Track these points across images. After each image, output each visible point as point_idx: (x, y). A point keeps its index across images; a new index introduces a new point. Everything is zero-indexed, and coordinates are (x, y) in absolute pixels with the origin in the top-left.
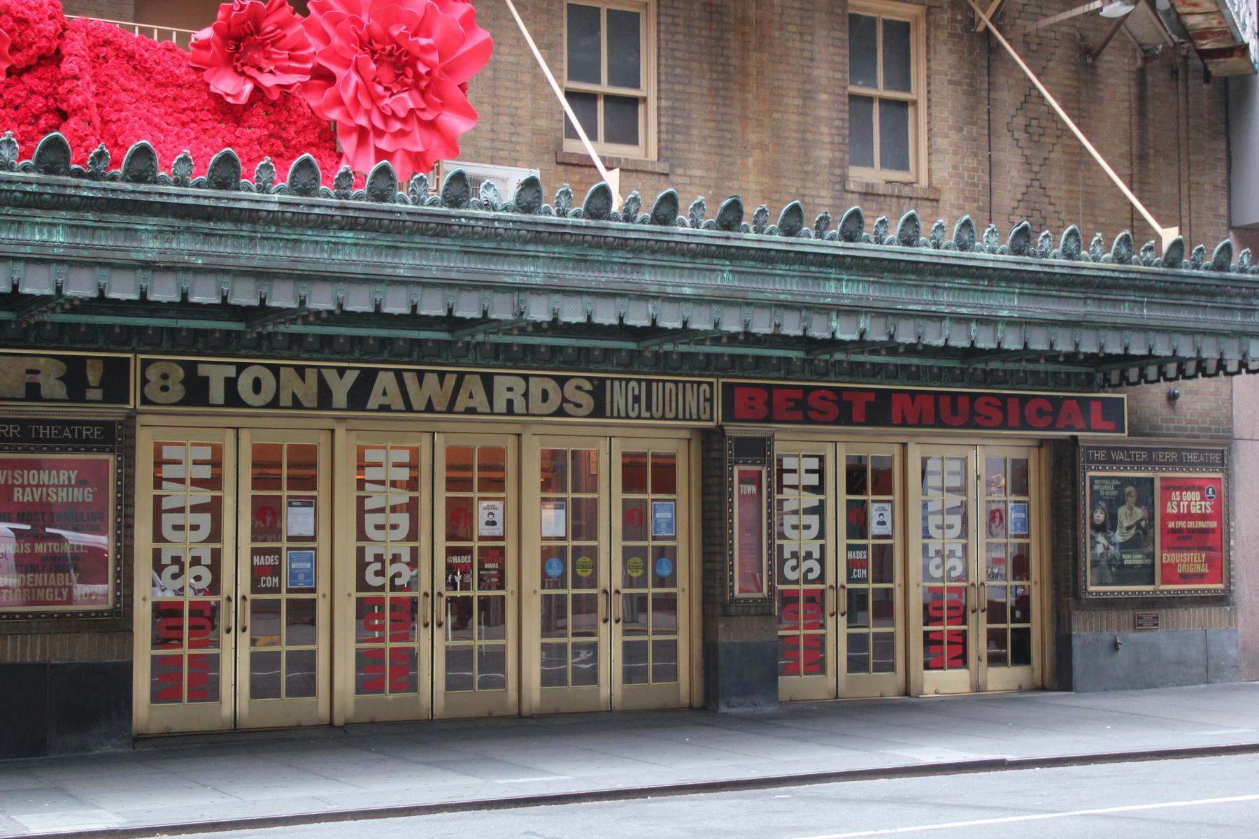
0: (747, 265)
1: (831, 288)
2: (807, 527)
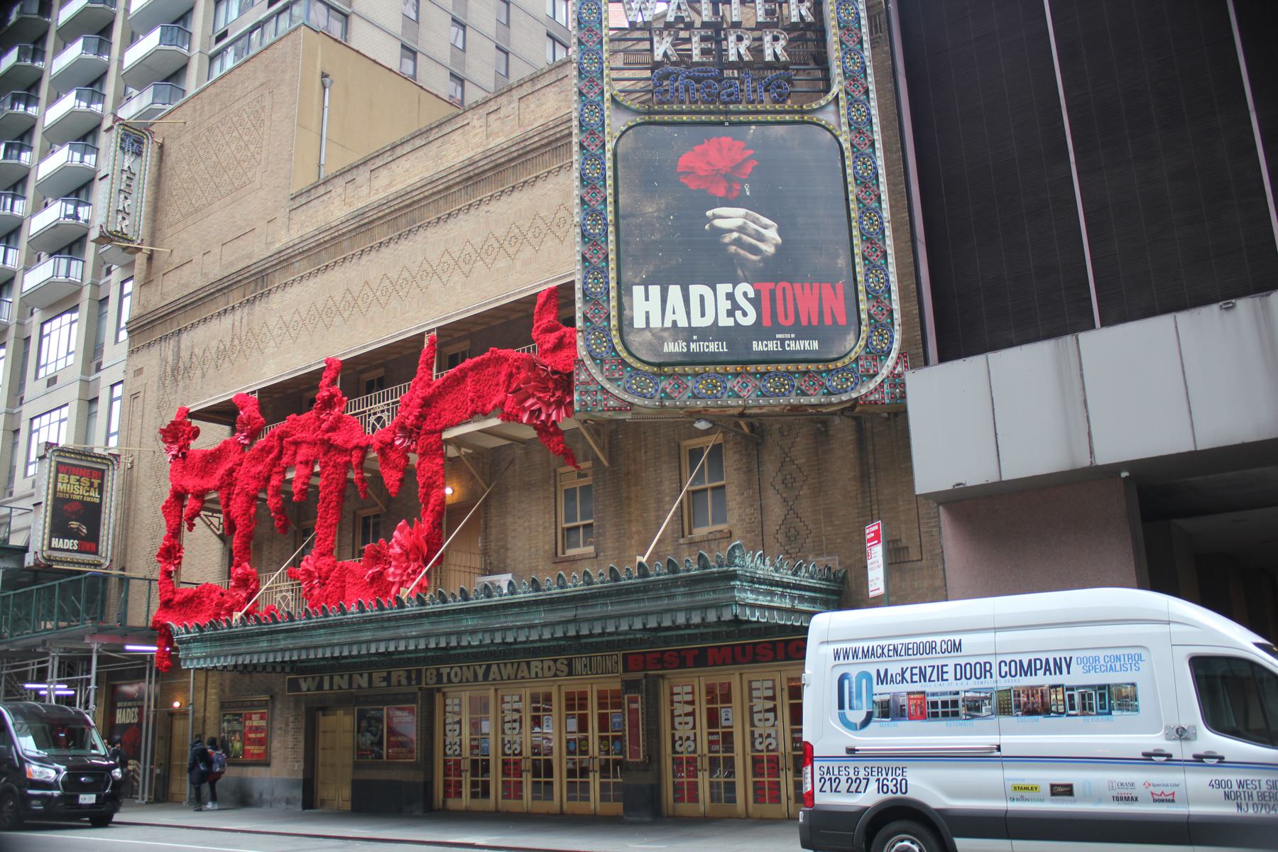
0: (433, 619)
1: (464, 623)
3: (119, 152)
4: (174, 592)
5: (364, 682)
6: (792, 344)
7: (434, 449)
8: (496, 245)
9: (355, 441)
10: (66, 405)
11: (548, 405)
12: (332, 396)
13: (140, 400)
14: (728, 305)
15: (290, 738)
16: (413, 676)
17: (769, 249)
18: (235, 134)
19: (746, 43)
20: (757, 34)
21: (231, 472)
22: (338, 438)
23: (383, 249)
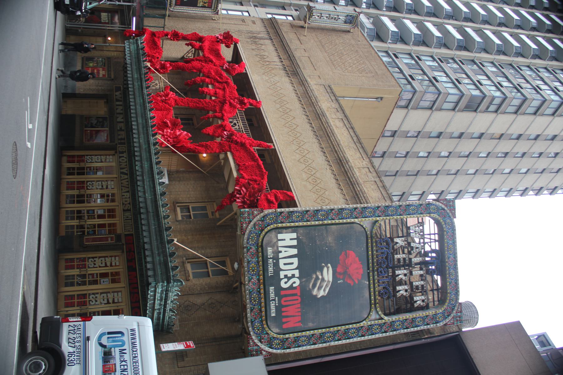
0: (147, 149)
1: (146, 163)
2: (102, 263)
3: (346, 14)
4: (159, 37)
5: (119, 119)
6: (273, 304)
7: (223, 149)
8: (312, 173)
9: (225, 114)
11: (243, 198)
12: (245, 104)
14: (290, 275)
15: (94, 87)
16: (122, 141)
17: (315, 292)
18: (356, 62)
19: (404, 278)
20: (408, 282)
21: (211, 61)
22: (227, 107)
23: (309, 125)
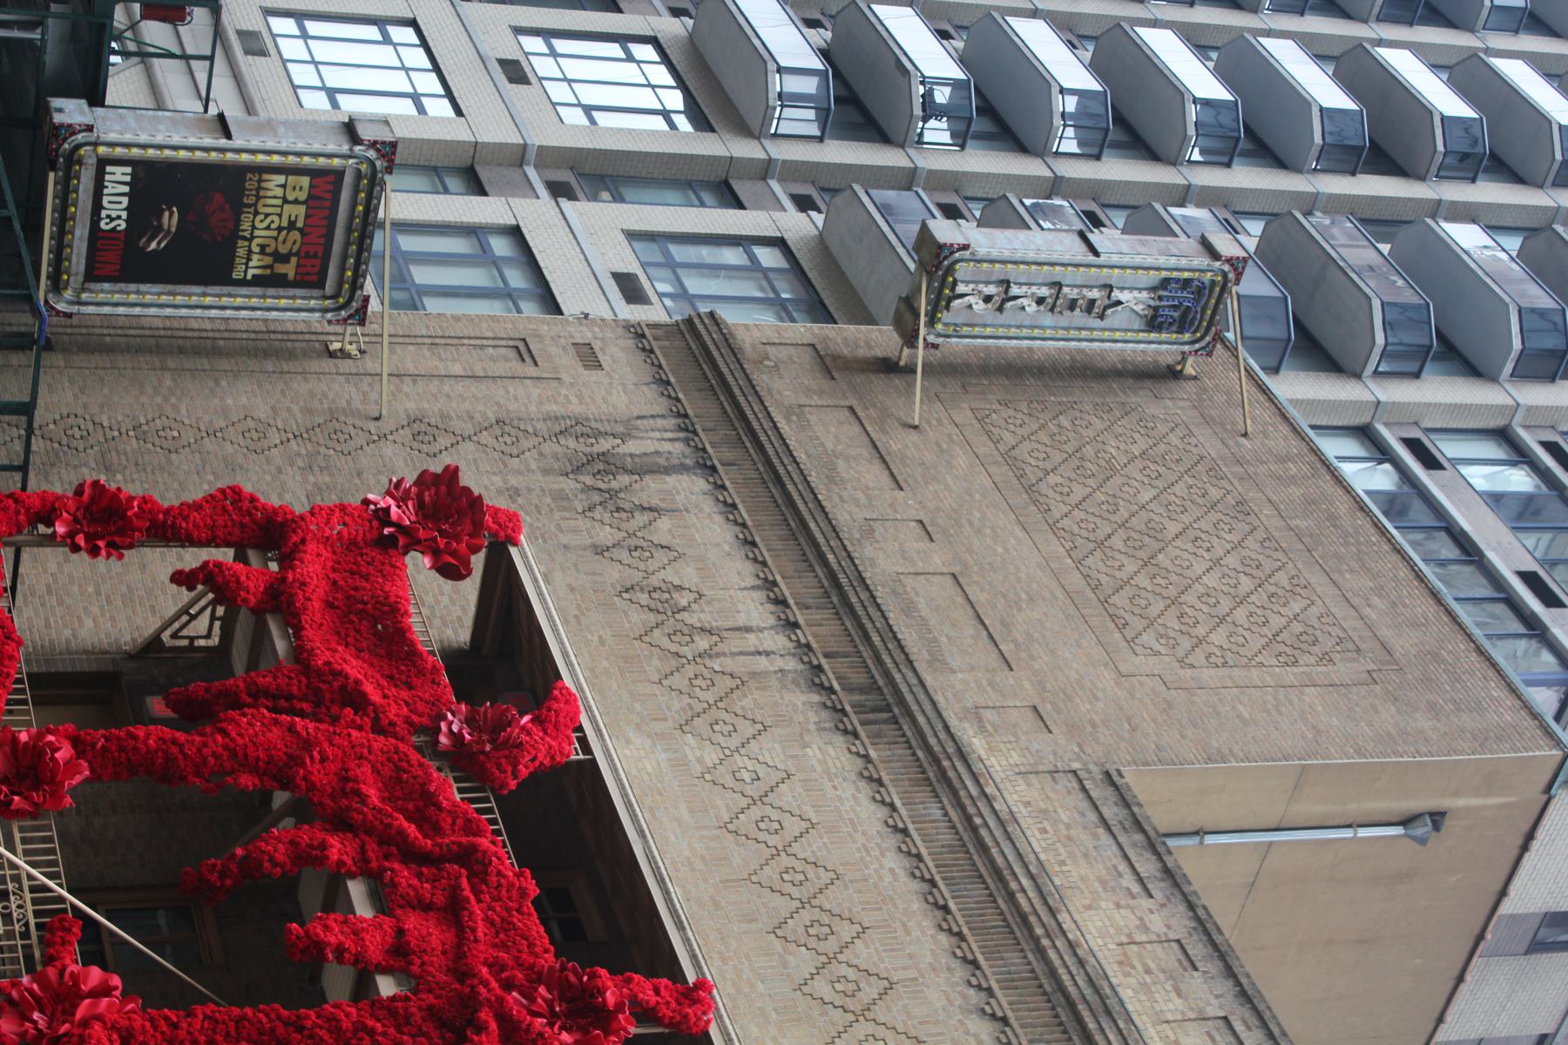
3: (1154, 277)
10: (459, 112)
13: (515, 366)
18: (1246, 584)
21: (354, 698)
